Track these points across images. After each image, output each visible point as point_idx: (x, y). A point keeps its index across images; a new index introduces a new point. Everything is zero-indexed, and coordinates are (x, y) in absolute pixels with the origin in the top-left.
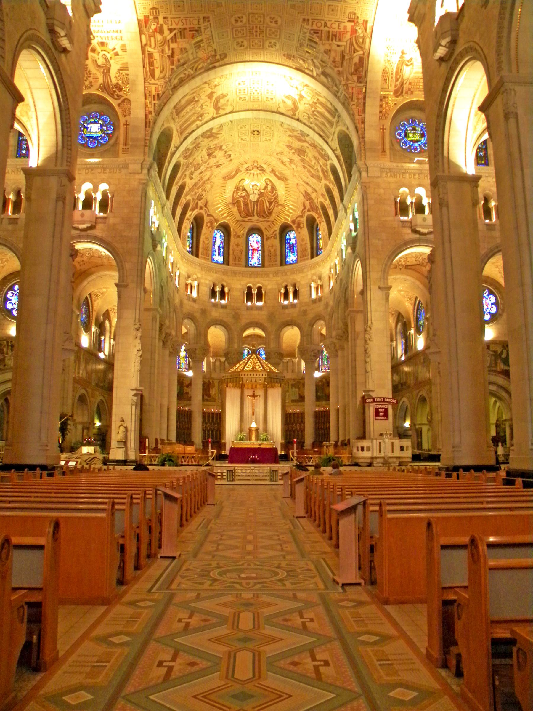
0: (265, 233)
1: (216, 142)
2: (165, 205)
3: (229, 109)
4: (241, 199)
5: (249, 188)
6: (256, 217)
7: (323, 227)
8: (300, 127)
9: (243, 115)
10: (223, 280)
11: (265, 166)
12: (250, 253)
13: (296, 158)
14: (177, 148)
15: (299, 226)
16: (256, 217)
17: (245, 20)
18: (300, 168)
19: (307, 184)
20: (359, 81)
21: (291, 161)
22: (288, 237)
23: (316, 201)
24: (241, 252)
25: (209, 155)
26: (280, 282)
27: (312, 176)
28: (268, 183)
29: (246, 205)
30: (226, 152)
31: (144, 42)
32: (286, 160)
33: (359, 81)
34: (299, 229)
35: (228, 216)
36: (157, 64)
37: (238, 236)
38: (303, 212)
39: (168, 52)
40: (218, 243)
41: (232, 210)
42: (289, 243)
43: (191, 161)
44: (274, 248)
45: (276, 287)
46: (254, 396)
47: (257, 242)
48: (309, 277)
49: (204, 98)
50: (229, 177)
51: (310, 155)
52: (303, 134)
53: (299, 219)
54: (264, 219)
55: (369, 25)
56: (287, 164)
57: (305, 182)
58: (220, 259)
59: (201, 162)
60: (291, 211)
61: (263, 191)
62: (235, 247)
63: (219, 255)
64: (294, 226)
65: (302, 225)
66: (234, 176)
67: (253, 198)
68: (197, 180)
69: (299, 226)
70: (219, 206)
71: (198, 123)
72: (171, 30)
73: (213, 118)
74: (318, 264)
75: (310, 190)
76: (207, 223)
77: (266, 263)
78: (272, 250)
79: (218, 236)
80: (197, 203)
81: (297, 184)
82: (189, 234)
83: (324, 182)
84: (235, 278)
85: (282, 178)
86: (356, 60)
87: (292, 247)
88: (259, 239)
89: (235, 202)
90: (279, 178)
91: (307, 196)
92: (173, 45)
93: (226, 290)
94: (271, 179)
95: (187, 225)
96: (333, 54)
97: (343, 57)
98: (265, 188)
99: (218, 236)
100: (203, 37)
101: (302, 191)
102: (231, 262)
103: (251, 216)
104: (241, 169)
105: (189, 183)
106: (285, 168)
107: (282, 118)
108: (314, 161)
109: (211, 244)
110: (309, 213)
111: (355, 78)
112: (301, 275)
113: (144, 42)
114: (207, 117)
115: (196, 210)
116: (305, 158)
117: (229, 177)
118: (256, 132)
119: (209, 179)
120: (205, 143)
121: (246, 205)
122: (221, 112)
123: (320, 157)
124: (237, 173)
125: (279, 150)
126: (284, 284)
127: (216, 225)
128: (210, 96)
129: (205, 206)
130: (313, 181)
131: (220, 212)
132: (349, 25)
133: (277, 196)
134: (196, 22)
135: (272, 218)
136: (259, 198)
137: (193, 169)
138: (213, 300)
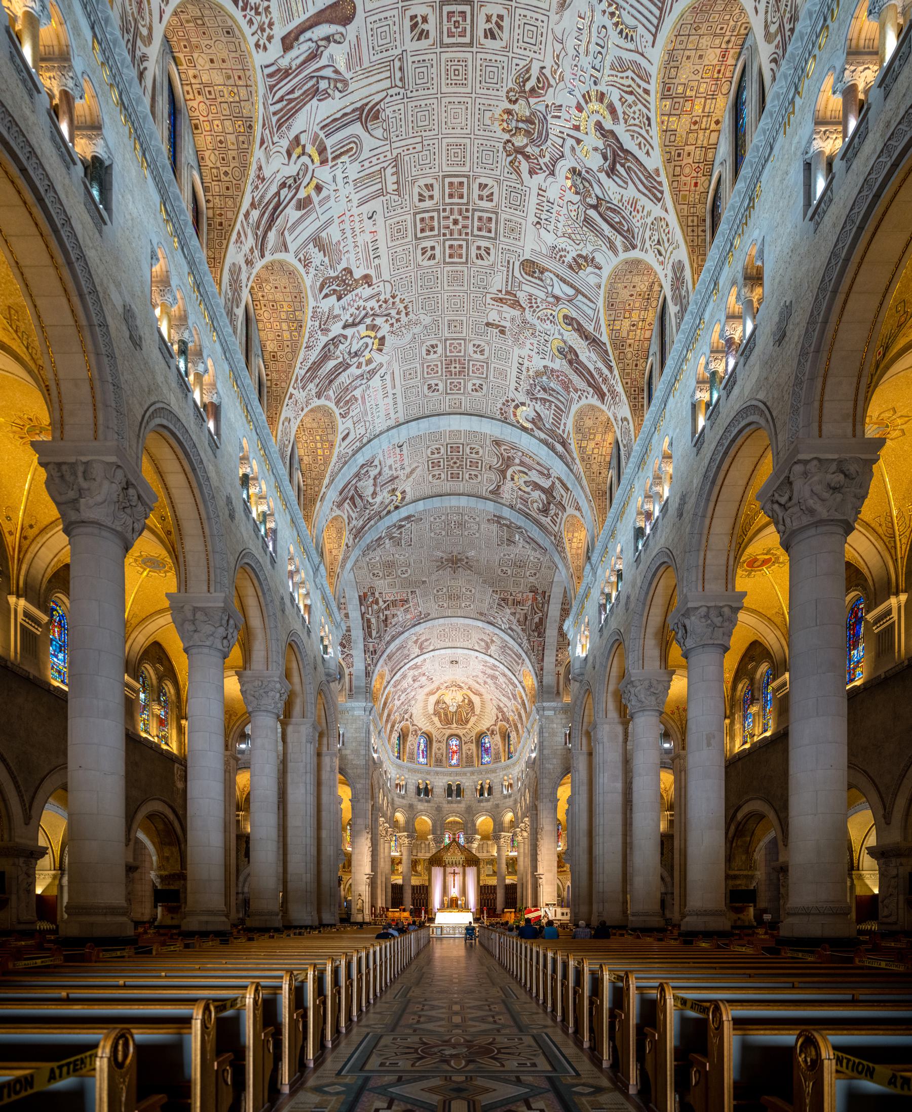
1: (420, 671)
3: (431, 648)
4: (442, 711)
6: (455, 725)
7: (513, 735)
8: (492, 661)
9: (443, 651)
11: (462, 685)
13: (489, 681)
14: (389, 682)
15: (492, 733)
16: (455, 725)
17: (445, 590)
18: (493, 688)
20: (539, 636)
21: (485, 683)
25: (414, 681)
29: (446, 715)
31: (363, 611)
32: (481, 681)
33: (539, 636)
36: (374, 626)
39: (382, 617)
40: (422, 746)
49: (410, 643)
50: (432, 693)
52: (494, 665)
55: (547, 594)
64: (489, 733)
67: (453, 709)
71: (406, 661)
72: (385, 602)
73: (418, 656)
75: (502, 705)
79: (422, 741)
83: (513, 701)
86: (537, 620)
89: (436, 713)
90: (475, 694)
91: (499, 709)
92: (386, 613)
95: (395, 735)
96: (517, 616)
97: (526, 618)
98: (463, 701)
100: (411, 604)
107: (477, 654)
108: (504, 686)
109: (416, 748)
111: (536, 634)
113: (363, 611)
114: (412, 656)
117: (432, 693)
118: (454, 662)
120: (411, 674)
121: (446, 715)
122: (425, 651)
124: (438, 690)
125: (474, 674)
127: (419, 733)
128: (416, 642)
130: (504, 699)
132: (531, 595)
134: (405, 595)
135: (469, 726)
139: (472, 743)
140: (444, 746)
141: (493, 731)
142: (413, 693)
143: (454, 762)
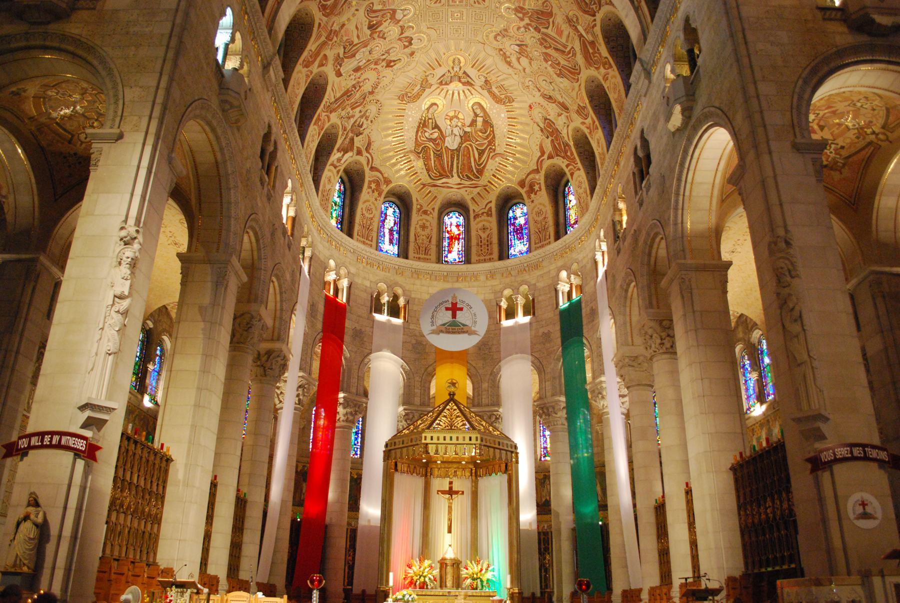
0: (472, 206)
2: (269, 64)
5: (444, 124)
6: (455, 180)
10: (397, 284)
11: (472, 73)
12: (446, 244)
15: (531, 190)
16: (455, 180)
18: (538, 63)
19: (550, 98)
22: (511, 214)
23: (564, 133)
24: (429, 238)
26: (498, 288)
27: (560, 75)
28: (478, 111)
29: (439, 156)
30: (402, 28)
34: (533, 196)
35: (407, 174)
37: (425, 212)
38: (539, 162)
40: (390, 222)
41: (414, 164)
42: (514, 224)
43: (336, 27)
44: (488, 232)
45: (492, 296)
46: (451, 492)
47: (458, 226)
48: (553, 273)
50: (408, 97)
51: (559, 19)
53: (531, 176)
54: (468, 183)
56: (513, 59)
57: (544, 96)
58: (394, 249)
59: (356, 41)
60: (517, 163)
61: (468, 129)
62: (419, 230)
63: (391, 242)
65: (536, 188)
66: (418, 96)
67: (452, 143)
68: (350, 83)
69: (531, 190)
70: (391, 154)
74: (570, 248)
76: (370, 182)
77: (474, 257)
78: (484, 236)
79: (390, 211)
80: (352, 140)
81: (530, 107)
82: (338, 200)
84: (418, 282)
85: (503, 99)
87: (519, 231)
88: (461, 220)
89: (421, 151)
93: (401, 302)
94: (483, 103)
98: (473, 123)
99: (390, 211)
101: (539, 118)
102: (411, 253)
103: (447, 177)
104: (432, 80)
105: (335, 87)
106: (510, 71)
110: (551, 161)
112: (538, 273)
115: (350, 154)
116: (549, 31)
119: (371, 93)
123: (580, 14)
126: (507, 292)
127: (385, 189)
129: (367, 150)
131: (394, 165)
133: (494, 137)
135: (483, 181)
136: (461, 143)
137: (341, 51)
138: (378, 317)
139: (489, 214)
140: (435, 223)
141: (531, 187)
142: (371, 75)
143: (453, 256)
